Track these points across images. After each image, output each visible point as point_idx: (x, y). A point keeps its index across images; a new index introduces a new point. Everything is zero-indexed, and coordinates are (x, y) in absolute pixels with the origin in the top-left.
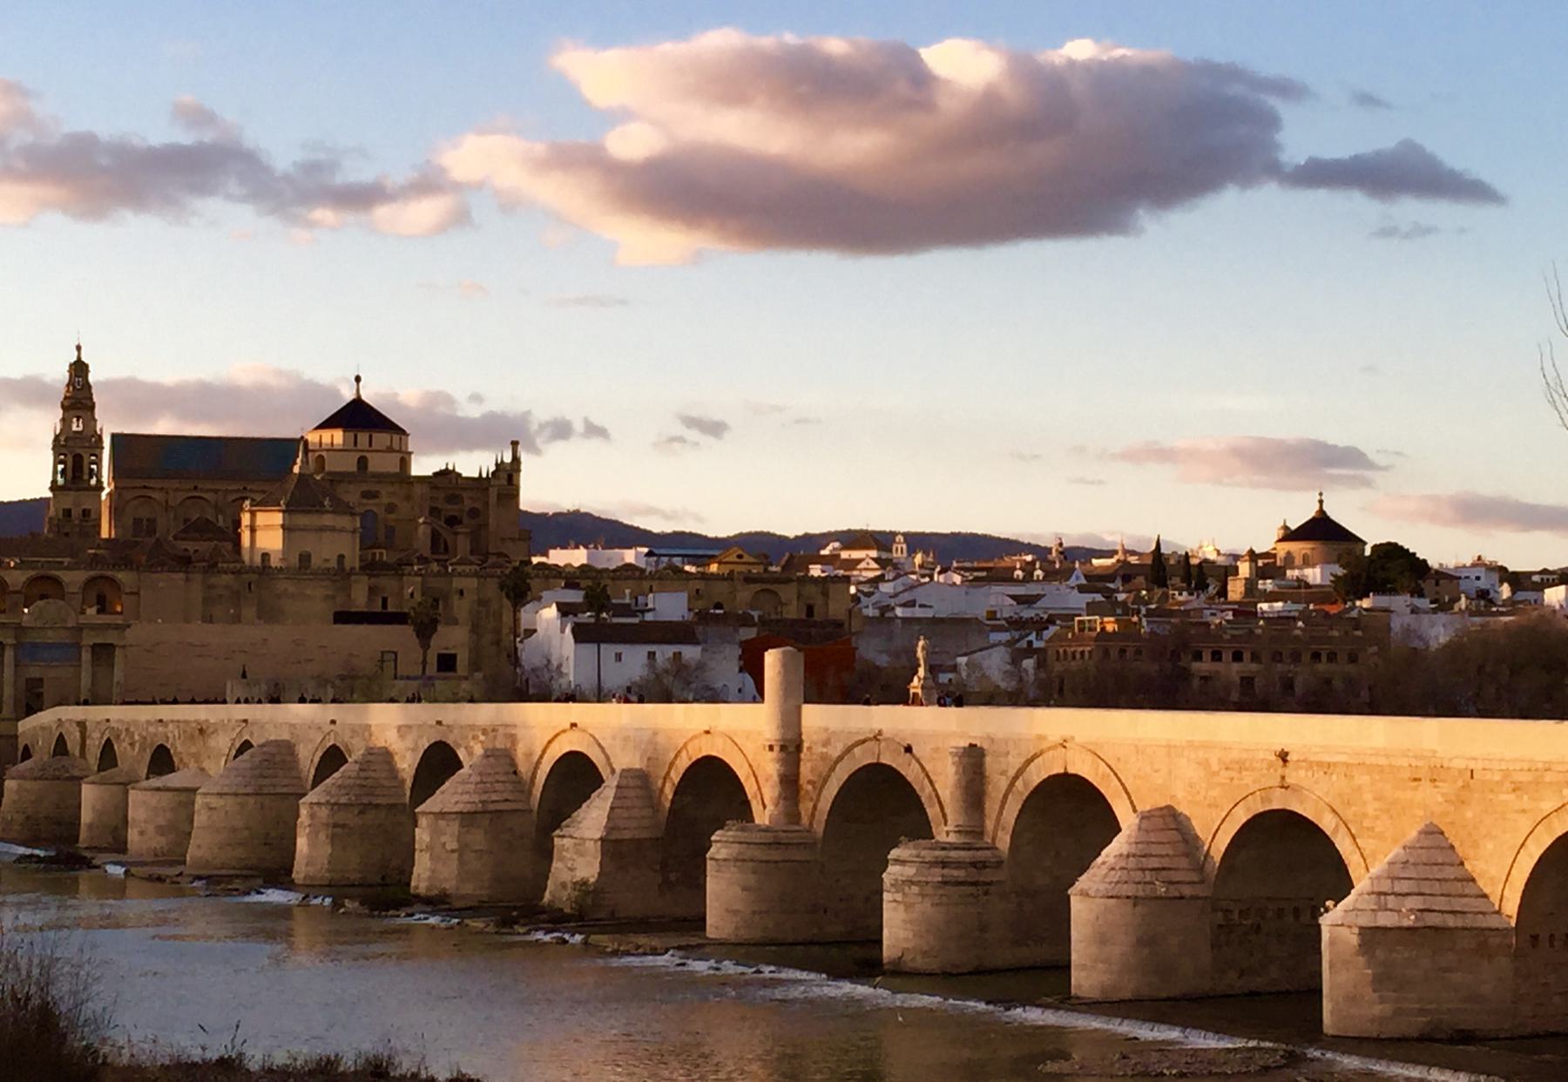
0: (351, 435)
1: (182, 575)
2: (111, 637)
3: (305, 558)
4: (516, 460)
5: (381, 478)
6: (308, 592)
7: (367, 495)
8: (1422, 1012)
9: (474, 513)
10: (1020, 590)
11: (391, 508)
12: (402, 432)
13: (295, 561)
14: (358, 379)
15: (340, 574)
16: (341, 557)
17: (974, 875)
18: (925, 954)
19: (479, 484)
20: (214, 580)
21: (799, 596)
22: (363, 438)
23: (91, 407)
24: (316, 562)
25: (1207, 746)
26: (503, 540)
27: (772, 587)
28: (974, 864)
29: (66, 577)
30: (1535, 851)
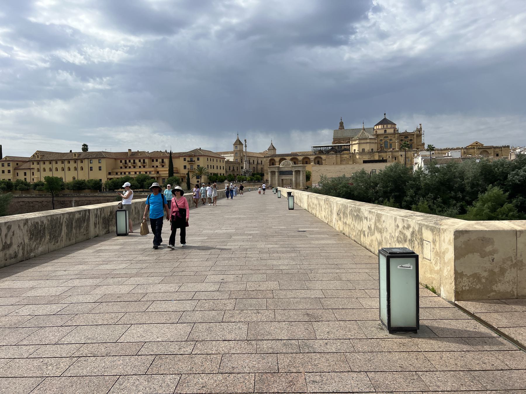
1: (335, 155)
3: (363, 150)
4: (421, 128)
6: (364, 157)
7: (385, 137)
9: (411, 140)
11: (391, 140)
13: (361, 150)
14: (385, 114)
16: (372, 149)
19: (412, 134)
20: (343, 156)
22: (385, 126)
24: (366, 150)
26: (418, 145)
27: (487, 150)
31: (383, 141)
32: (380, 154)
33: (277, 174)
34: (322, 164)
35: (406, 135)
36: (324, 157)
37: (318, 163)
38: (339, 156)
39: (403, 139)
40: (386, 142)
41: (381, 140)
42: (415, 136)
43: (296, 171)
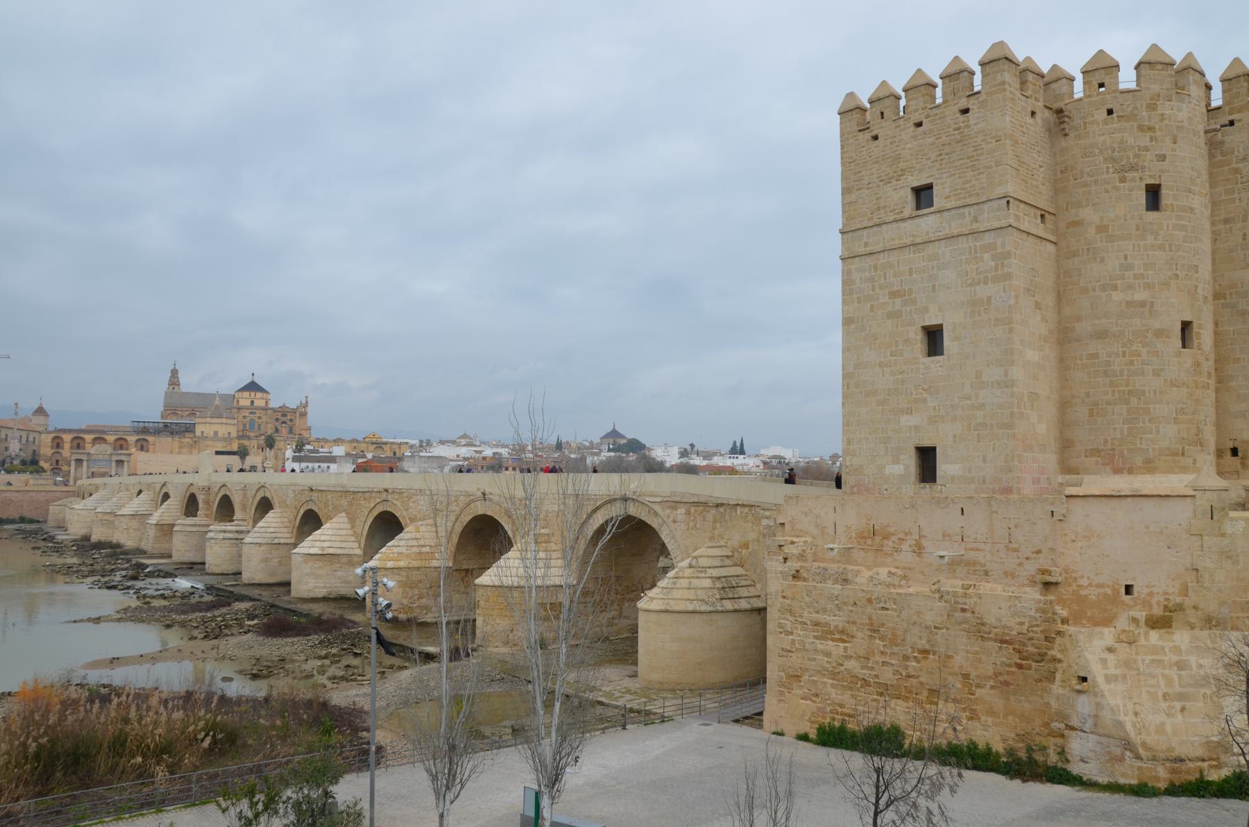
0: (248, 393)
1: (170, 439)
2: (123, 458)
3: (216, 433)
4: (307, 403)
5: (257, 408)
7: (251, 413)
8: (325, 587)
9: (291, 420)
10: (476, 449)
11: (260, 418)
12: (267, 392)
14: (253, 374)
15: (228, 439)
17: (237, 536)
18: (216, 566)
19: (294, 411)
21: (391, 448)
22: (253, 394)
23: (179, 385)
25: (295, 485)
28: (237, 532)
29: (128, 438)
30: (369, 523)
31: (248, 419)
32: (241, 442)
33: (85, 463)
34: (148, 451)
35: (284, 411)
36: (151, 439)
37: (142, 449)
38: (177, 439)
39: (279, 417)
40: (252, 421)
41: (245, 417)
42: (298, 413)
43: (117, 461)
